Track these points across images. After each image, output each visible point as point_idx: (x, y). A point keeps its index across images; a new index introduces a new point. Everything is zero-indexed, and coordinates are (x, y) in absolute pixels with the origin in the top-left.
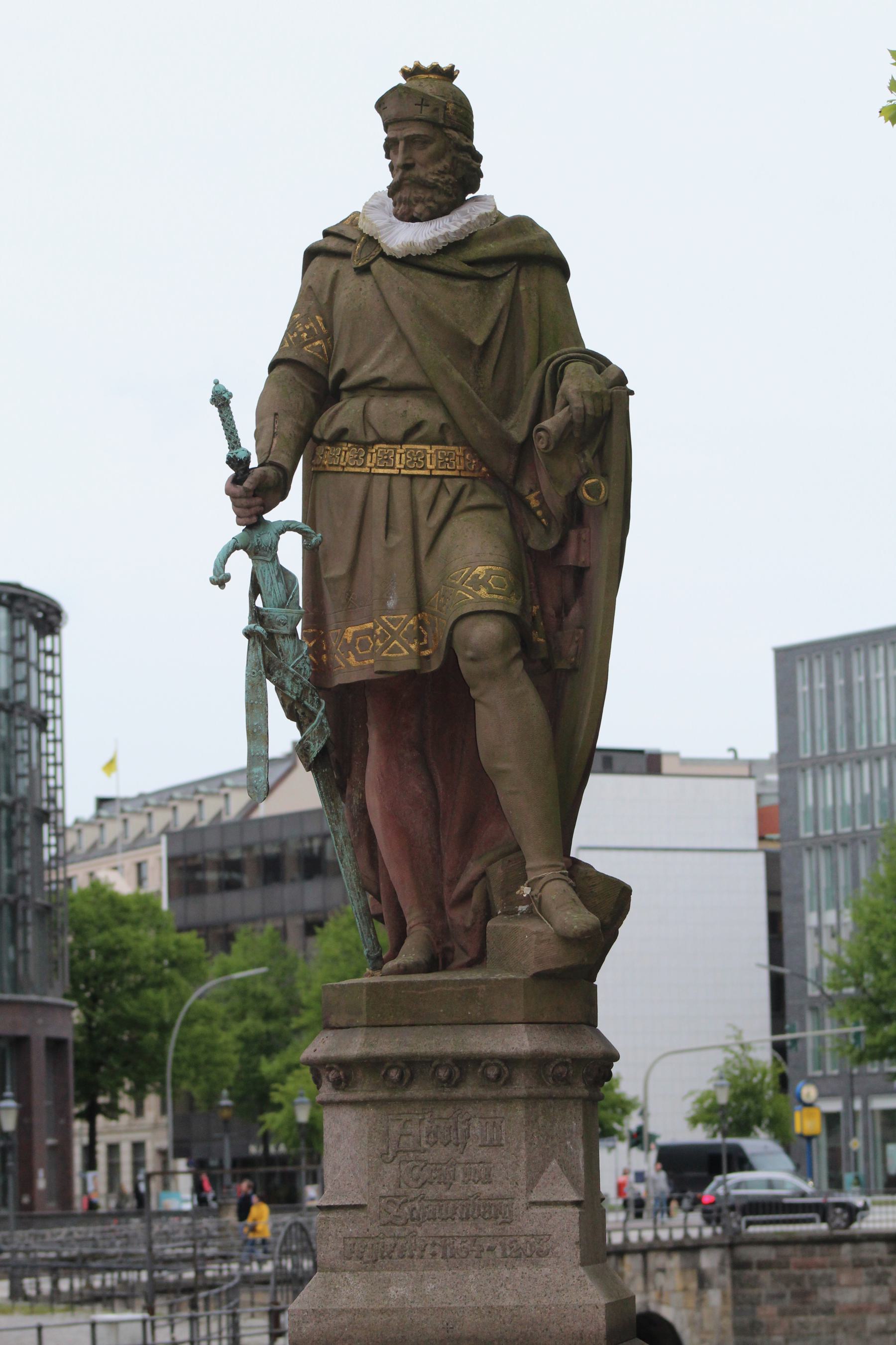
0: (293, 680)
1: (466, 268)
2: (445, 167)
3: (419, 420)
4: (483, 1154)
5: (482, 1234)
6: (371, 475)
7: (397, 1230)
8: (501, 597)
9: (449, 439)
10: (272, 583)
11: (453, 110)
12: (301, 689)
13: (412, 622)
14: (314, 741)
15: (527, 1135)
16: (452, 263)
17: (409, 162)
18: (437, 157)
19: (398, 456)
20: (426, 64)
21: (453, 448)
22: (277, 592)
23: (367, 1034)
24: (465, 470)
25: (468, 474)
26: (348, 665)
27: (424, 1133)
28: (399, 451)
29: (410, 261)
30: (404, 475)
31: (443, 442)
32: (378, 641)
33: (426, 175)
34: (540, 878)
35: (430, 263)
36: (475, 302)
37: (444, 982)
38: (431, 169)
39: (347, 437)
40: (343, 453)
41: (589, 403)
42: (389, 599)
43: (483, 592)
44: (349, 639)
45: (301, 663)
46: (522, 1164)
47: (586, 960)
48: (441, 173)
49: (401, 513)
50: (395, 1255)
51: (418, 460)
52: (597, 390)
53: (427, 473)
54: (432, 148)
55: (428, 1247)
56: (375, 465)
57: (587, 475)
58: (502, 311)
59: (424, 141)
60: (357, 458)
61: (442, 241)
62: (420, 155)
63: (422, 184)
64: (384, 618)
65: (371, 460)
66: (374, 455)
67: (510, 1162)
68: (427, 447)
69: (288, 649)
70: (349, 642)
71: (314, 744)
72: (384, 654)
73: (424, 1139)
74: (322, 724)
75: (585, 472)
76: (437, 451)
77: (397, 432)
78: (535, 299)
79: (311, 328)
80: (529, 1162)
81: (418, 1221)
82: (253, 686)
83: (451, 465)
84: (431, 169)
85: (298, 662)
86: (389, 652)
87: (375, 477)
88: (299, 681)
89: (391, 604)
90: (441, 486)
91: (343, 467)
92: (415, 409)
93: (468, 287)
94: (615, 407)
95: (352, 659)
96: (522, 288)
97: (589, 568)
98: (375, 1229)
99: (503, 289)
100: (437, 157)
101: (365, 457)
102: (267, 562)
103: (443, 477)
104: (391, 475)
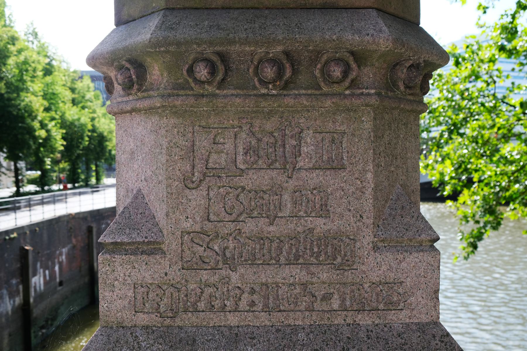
4: (315, 178)
5: (315, 280)
7: (205, 275)
15: (374, 153)
23: (164, 16)
27: (241, 149)
46: (369, 193)
50: (201, 305)
55: (246, 295)
67: (352, 189)
73: (240, 158)
80: (375, 190)
81: (230, 262)
98: (175, 274)
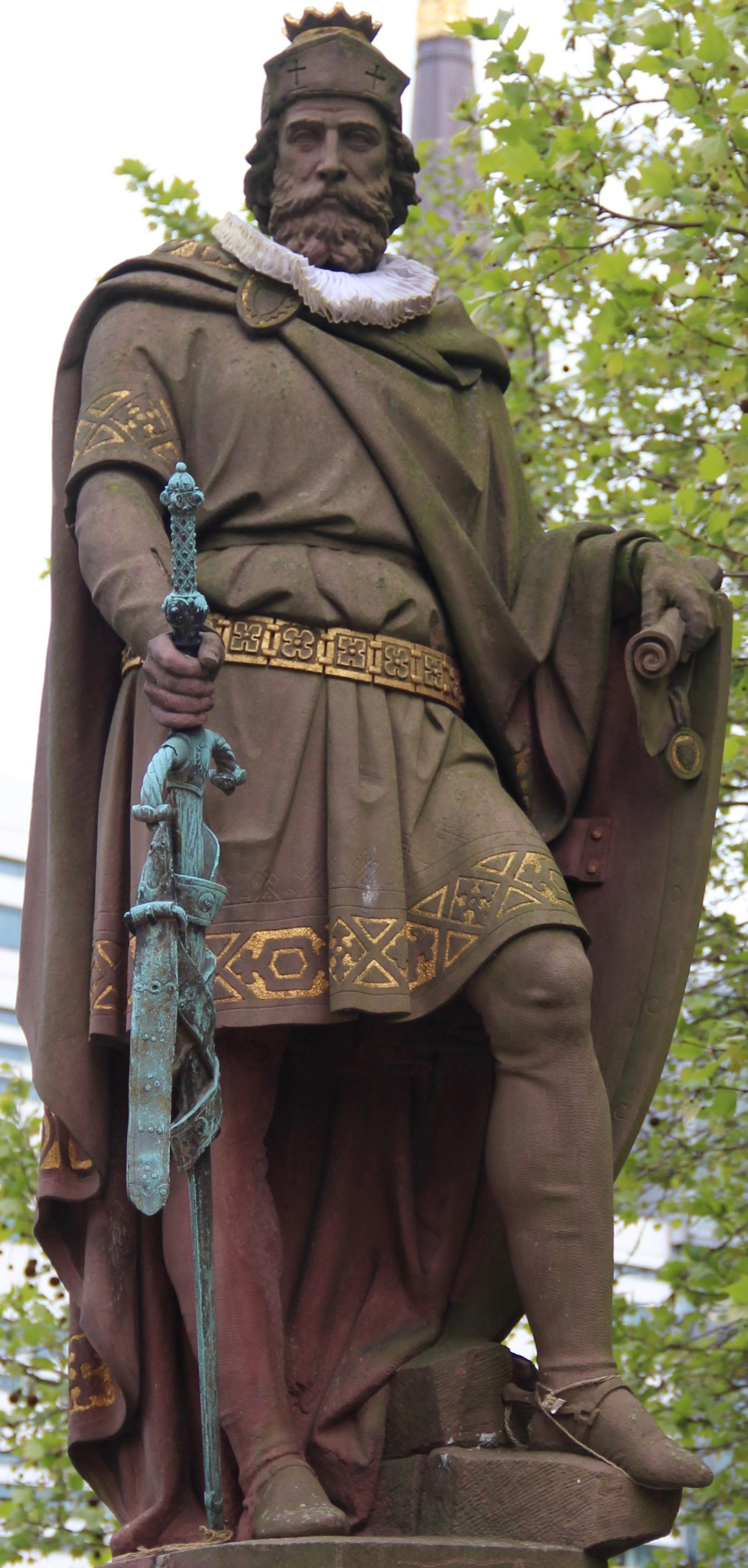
3: (406, 597)
14: (209, 1119)
18: (375, 171)
20: (326, 9)
26: (248, 996)
32: (347, 958)
34: (596, 1384)
35: (386, 342)
37: (462, 1549)
39: (281, 608)
40: (267, 635)
44: (257, 954)
49: (383, 749)
60: (300, 646)
65: (324, 653)
66: (331, 645)
69: (199, 953)
70: (256, 956)
77: (375, 612)
82: (150, 1009)
87: (332, 682)
89: (368, 898)
91: (269, 658)
95: (259, 987)
97: (598, 885)
101: (314, 646)
102: (198, 796)
104: (358, 683)
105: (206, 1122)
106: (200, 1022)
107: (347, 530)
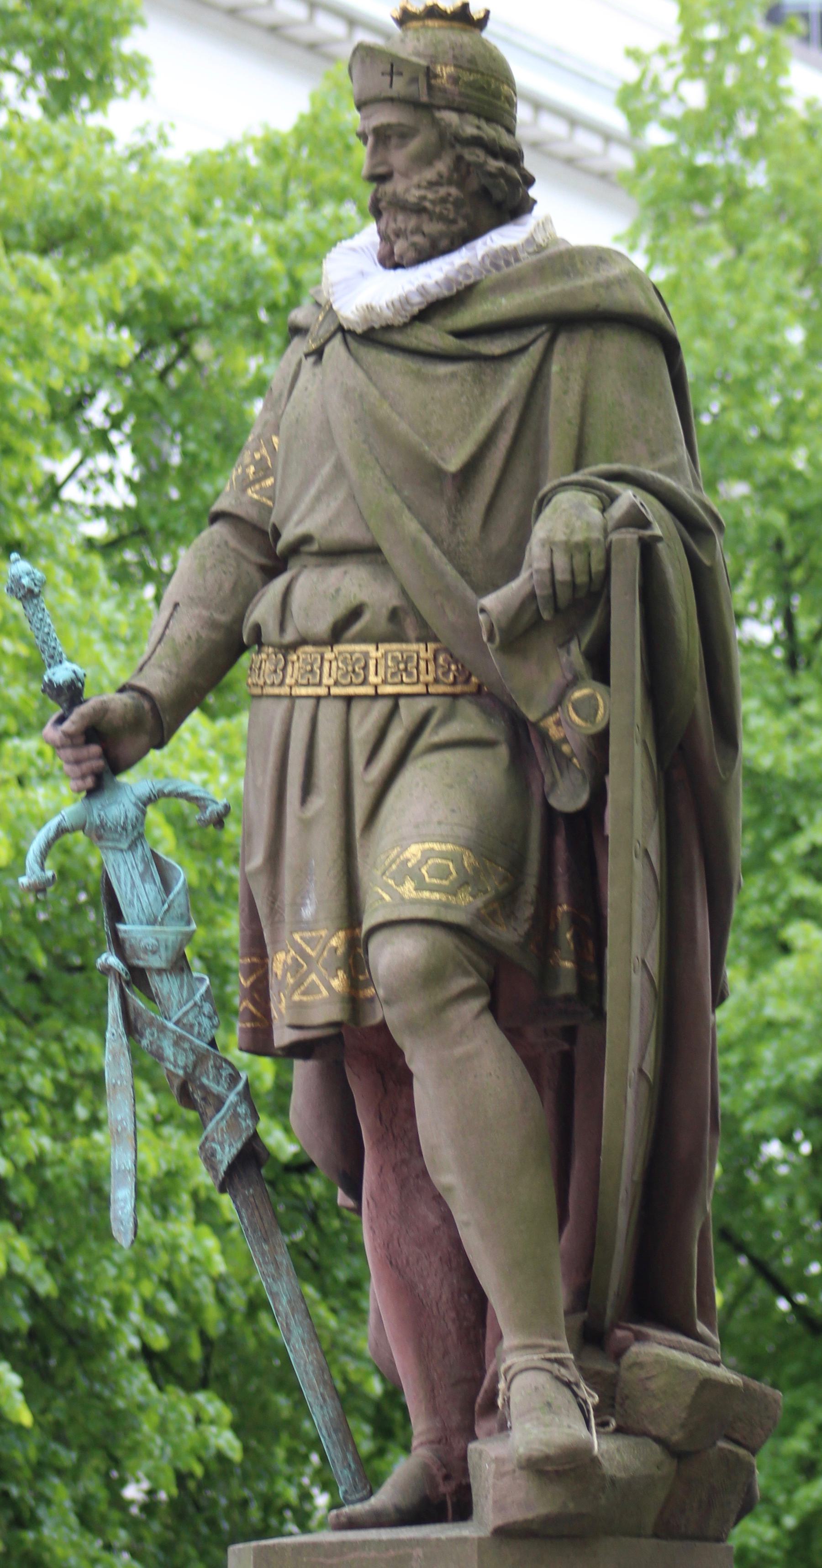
0: (176, 1044)
1: (450, 343)
2: (440, 176)
3: (355, 602)
6: (292, 698)
8: (436, 896)
9: (411, 632)
10: (133, 885)
11: (450, 76)
12: (192, 1058)
13: (334, 942)
16: (430, 336)
17: (381, 170)
18: (425, 159)
19: (326, 665)
21: (414, 647)
22: (144, 899)
24: (436, 681)
25: (441, 689)
28: (329, 655)
29: (373, 337)
30: (337, 697)
31: (398, 637)
33: (407, 190)
35: (398, 338)
36: (463, 399)
38: (416, 179)
41: (561, 561)
42: (304, 905)
43: (408, 889)
45: (191, 1017)
47: (571, 1506)
48: (431, 185)
51: (358, 670)
52: (579, 537)
53: (370, 691)
54: (414, 145)
56: (297, 681)
57: (574, 682)
58: (504, 412)
59: (404, 134)
61: (416, 299)
62: (399, 158)
63: (400, 206)
64: (297, 937)
68: (371, 648)
69: (170, 992)
71: (223, 1149)
72: (296, 997)
74: (236, 1115)
75: (569, 676)
76: (385, 656)
77: (322, 626)
78: (576, 386)
79: (263, 458)
83: (410, 675)
84: (416, 179)
85: (186, 1014)
86: (304, 993)
88: (186, 1046)
89: (308, 912)
90: (394, 711)
92: (352, 583)
93: (453, 375)
94: (614, 565)
96: (555, 368)
99: (518, 373)
100: (425, 159)
102: (122, 851)
103: (397, 697)
104: (318, 698)
105: (218, 1148)
106: (172, 1059)
107: (315, 547)
